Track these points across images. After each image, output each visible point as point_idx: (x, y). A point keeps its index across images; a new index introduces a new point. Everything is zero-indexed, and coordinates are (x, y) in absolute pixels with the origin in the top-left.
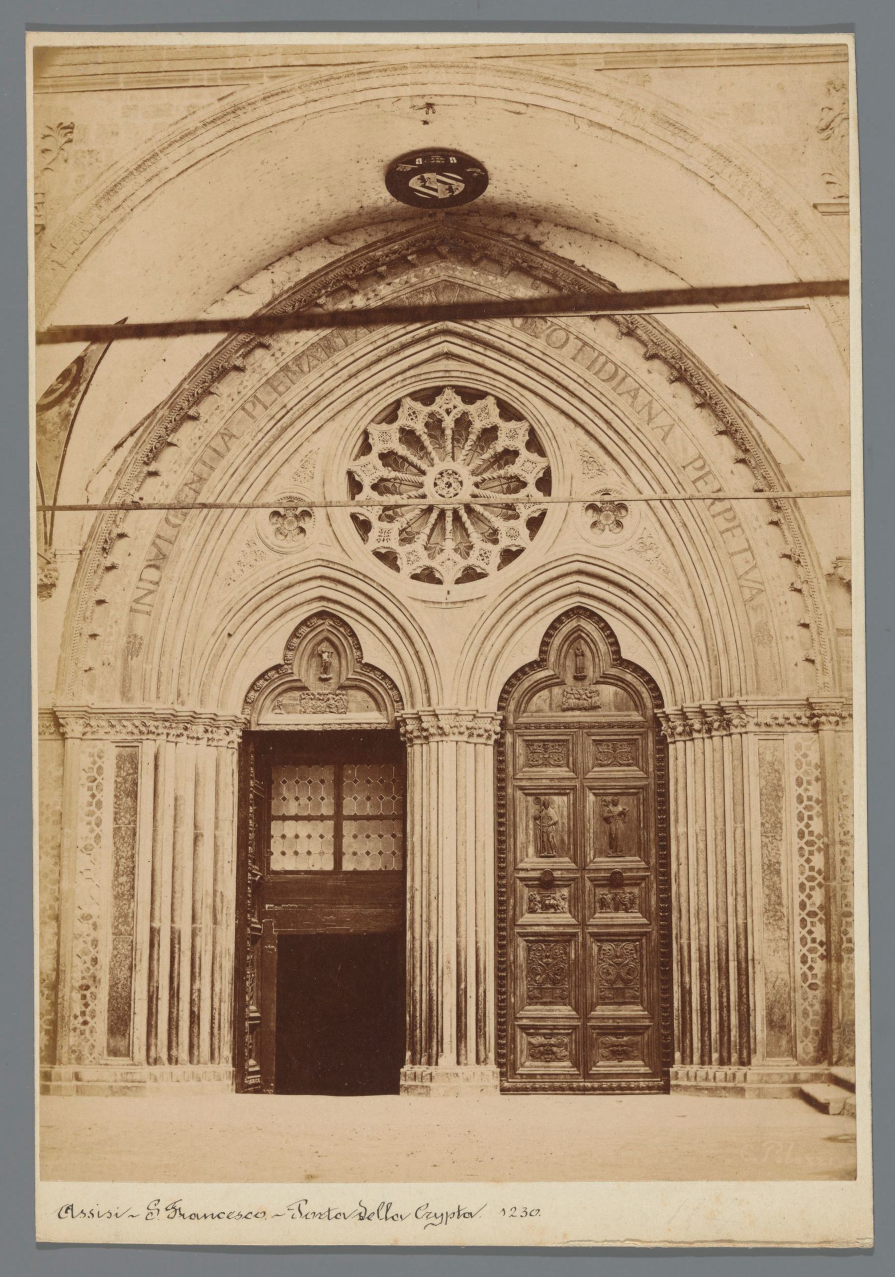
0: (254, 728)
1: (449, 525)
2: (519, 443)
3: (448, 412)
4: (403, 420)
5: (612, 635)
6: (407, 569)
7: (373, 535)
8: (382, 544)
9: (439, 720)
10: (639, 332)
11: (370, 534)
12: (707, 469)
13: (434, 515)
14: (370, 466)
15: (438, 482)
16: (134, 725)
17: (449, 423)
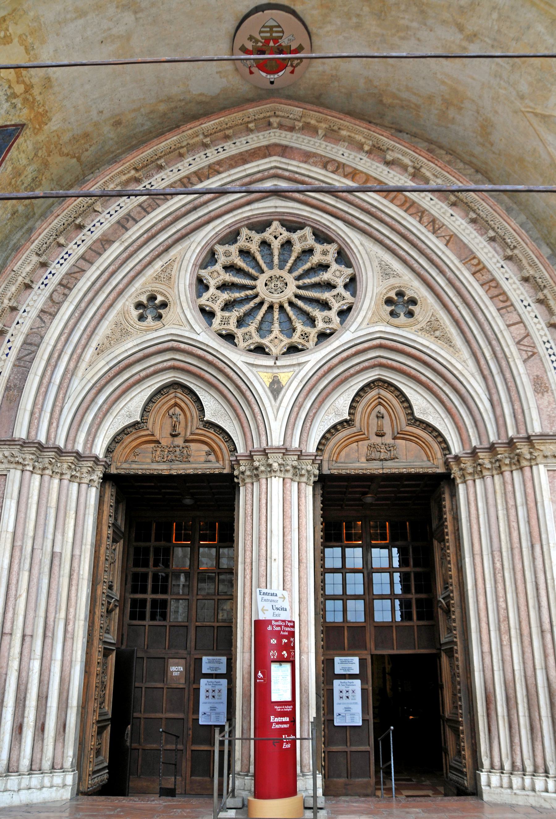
0: (113, 471)
1: (276, 314)
2: (330, 258)
3: (276, 238)
4: (242, 242)
5: (407, 400)
6: (242, 345)
7: (216, 321)
8: (223, 327)
9: (268, 458)
10: (423, 170)
11: (214, 320)
12: (481, 266)
13: (265, 307)
14: (215, 273)
15: (268, 283)
16: (4, 455)
17: (276, 245)
